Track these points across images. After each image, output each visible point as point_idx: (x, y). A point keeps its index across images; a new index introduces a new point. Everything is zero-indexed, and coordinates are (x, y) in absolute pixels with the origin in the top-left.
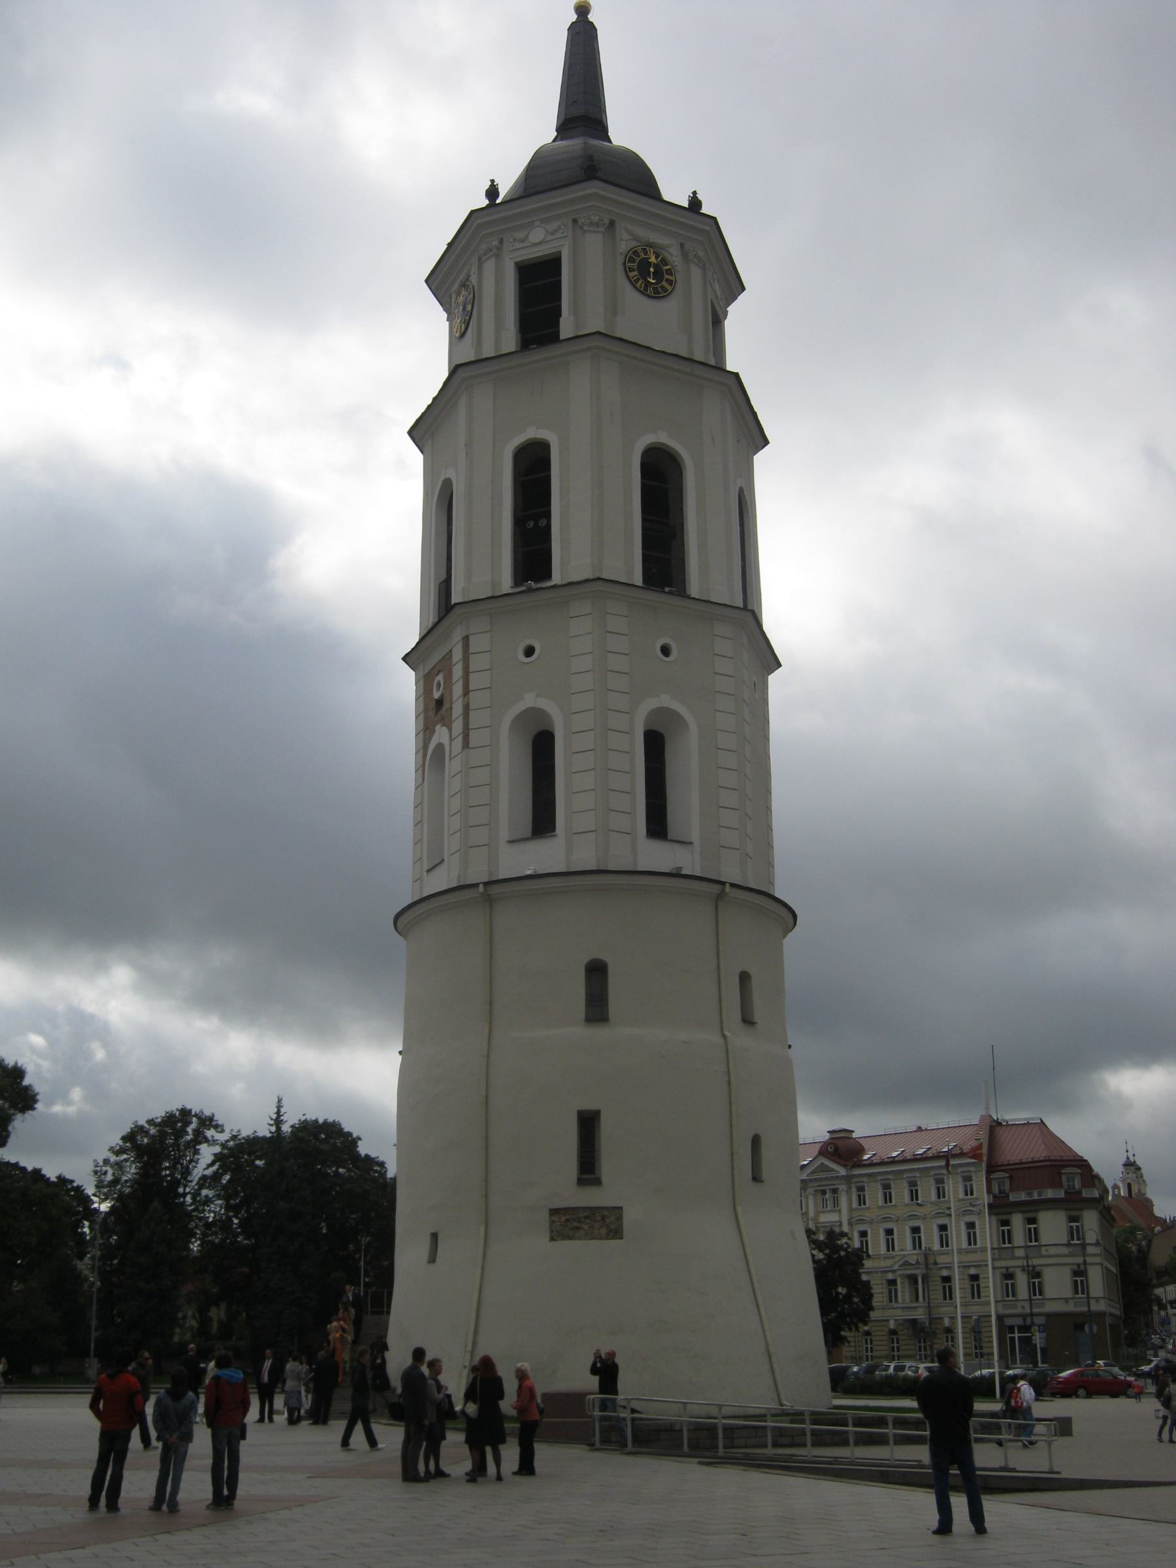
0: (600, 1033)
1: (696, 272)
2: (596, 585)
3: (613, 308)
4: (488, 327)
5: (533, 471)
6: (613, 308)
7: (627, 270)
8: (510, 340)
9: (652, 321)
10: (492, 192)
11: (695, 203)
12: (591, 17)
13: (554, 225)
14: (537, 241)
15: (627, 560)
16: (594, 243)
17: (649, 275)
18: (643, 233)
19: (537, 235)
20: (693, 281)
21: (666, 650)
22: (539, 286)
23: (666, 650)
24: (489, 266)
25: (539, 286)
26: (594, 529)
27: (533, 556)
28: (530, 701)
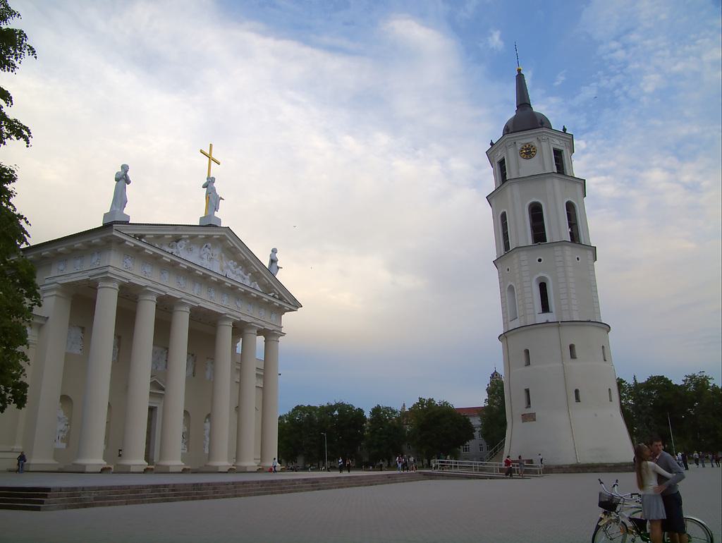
5: (570, 207)
19: (558, 142)
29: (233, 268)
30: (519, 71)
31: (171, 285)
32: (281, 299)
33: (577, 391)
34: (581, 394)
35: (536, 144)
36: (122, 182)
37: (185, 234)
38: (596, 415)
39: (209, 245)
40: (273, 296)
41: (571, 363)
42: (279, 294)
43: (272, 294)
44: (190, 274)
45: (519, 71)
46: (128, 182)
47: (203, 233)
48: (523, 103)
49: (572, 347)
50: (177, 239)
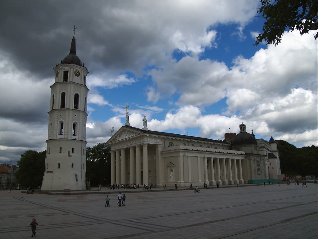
1: (83, 73)
3: (73, 78)
5: (63, 95)
6: (73, 78)
7: (75, 73)
8: (62, 80)
9: (77, 80)
10: (61, 62)
11: (84, 65)
15: (72, 107)
16: (72, 70)
17: (77, 74)
20: (82, 74)
22: (66, 74)
23: (76, 116)
24: (60, 71)
25: (66, 74)
26: (70, 103)
28: (61, 120)
34: (74, 165)
45: (74, 37)
48: (73, 51)
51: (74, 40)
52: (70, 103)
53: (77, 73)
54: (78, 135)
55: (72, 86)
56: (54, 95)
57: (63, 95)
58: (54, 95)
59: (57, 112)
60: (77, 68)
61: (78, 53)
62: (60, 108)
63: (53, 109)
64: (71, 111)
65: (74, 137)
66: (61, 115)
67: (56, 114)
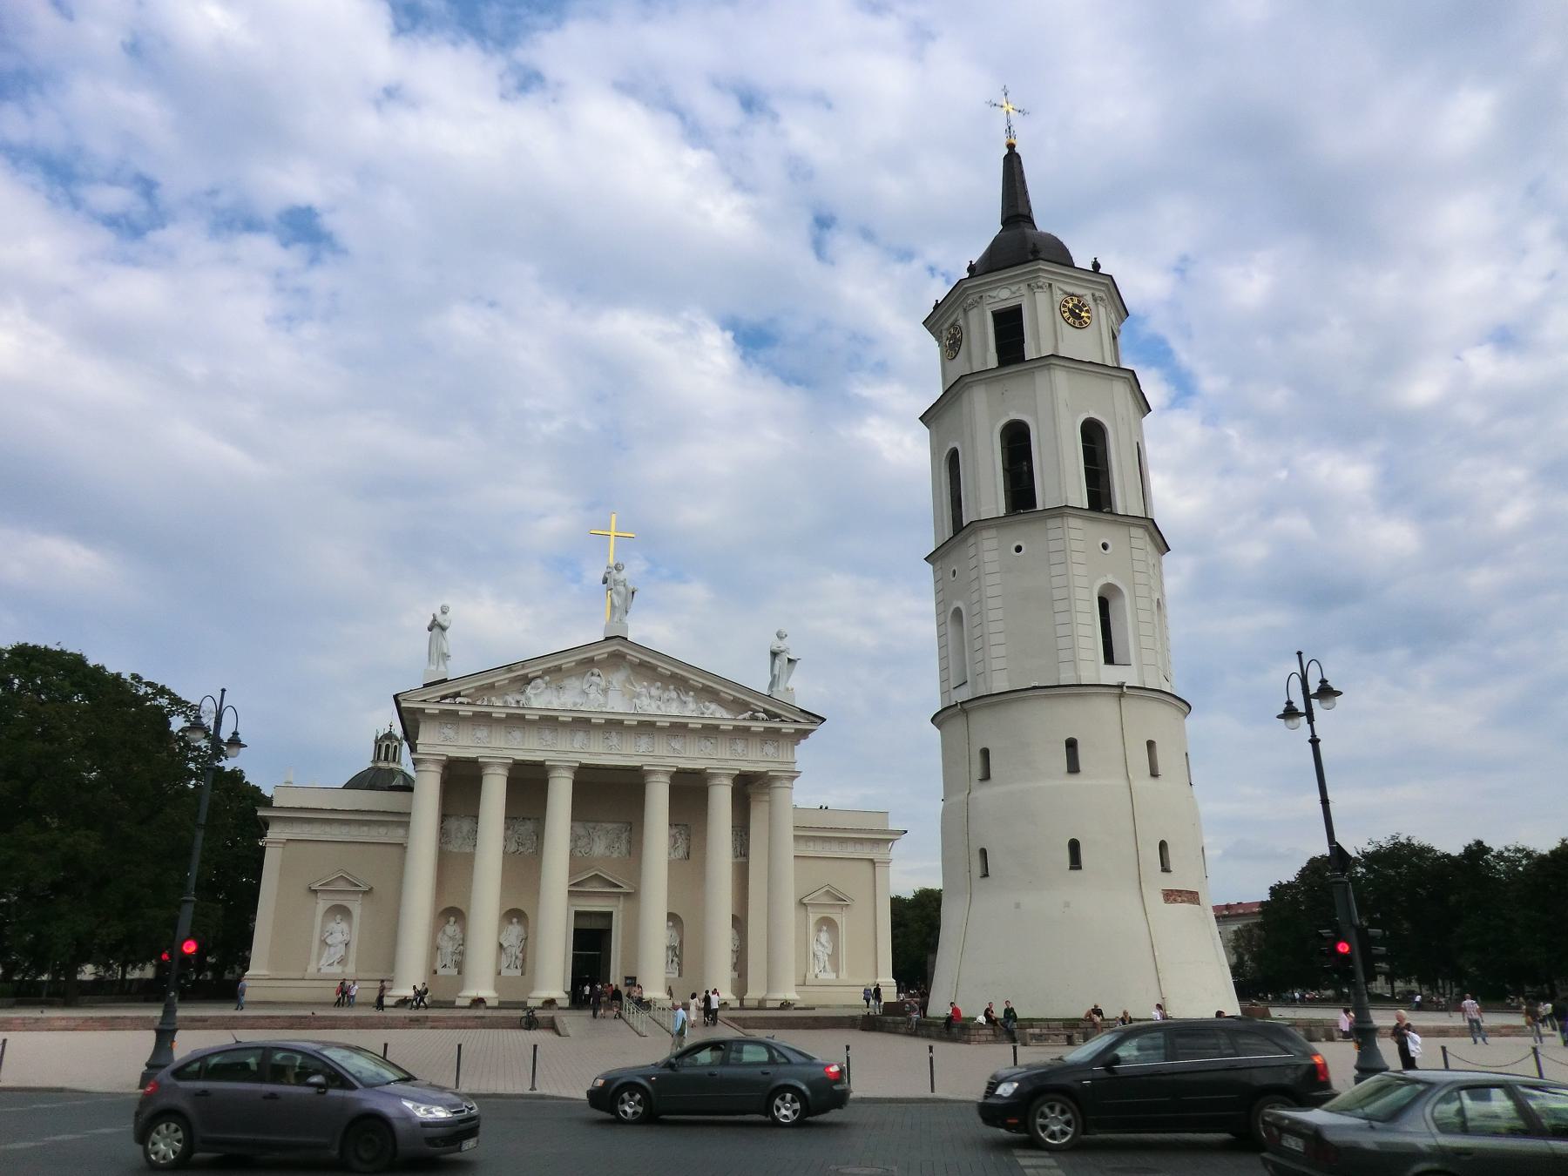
0: (1074, 780)
1: (1102, 310)
2: (1062, 511)
4: (976, 350)
8: (993, 361)
10: (971, 269)
11: (1096, 266)
12: (1017, 149)
13: (1014, 288)
14: (1003, 296)
17: (1076, 315)
18: (1070, 289)
19: (1004, 293)
20: (1102, 316)
21: (1105, 546)
23: (1105, 546)
27: (1021, 494)
29: (654, 692)
30: (1011, 147)
31: (529, 747)
32: (772, 716)
33: (983, 852)
35: (961, 322)
36: (436, 630)
37: (531, 671)
38: (1018, 906)
39: (596, 671)
40: (756, 719)
41: (983, 793)
42: (766, 711)
43: (747, 715)
44: (549, 722)
45: (1011, 147)
46: (443, 629)
47: (600, 654)
49: (985, 753)
50: (527, 680)
51: (1012, 162)
52: (1060, 475)
53: (1071, 311)
54: (1133, 661)
55: (1060, 377)
56: (953, 457)
57: (1016, 441)
58: (953, 457)
59: (992, 533)
60: (1064, 287)
61: (1045, 220)
62: (1002, 511)
63: (958, 526)
64: (1074, 523)
65: (1111, 675)
66: (1019, 549)
67: (990, 549)
